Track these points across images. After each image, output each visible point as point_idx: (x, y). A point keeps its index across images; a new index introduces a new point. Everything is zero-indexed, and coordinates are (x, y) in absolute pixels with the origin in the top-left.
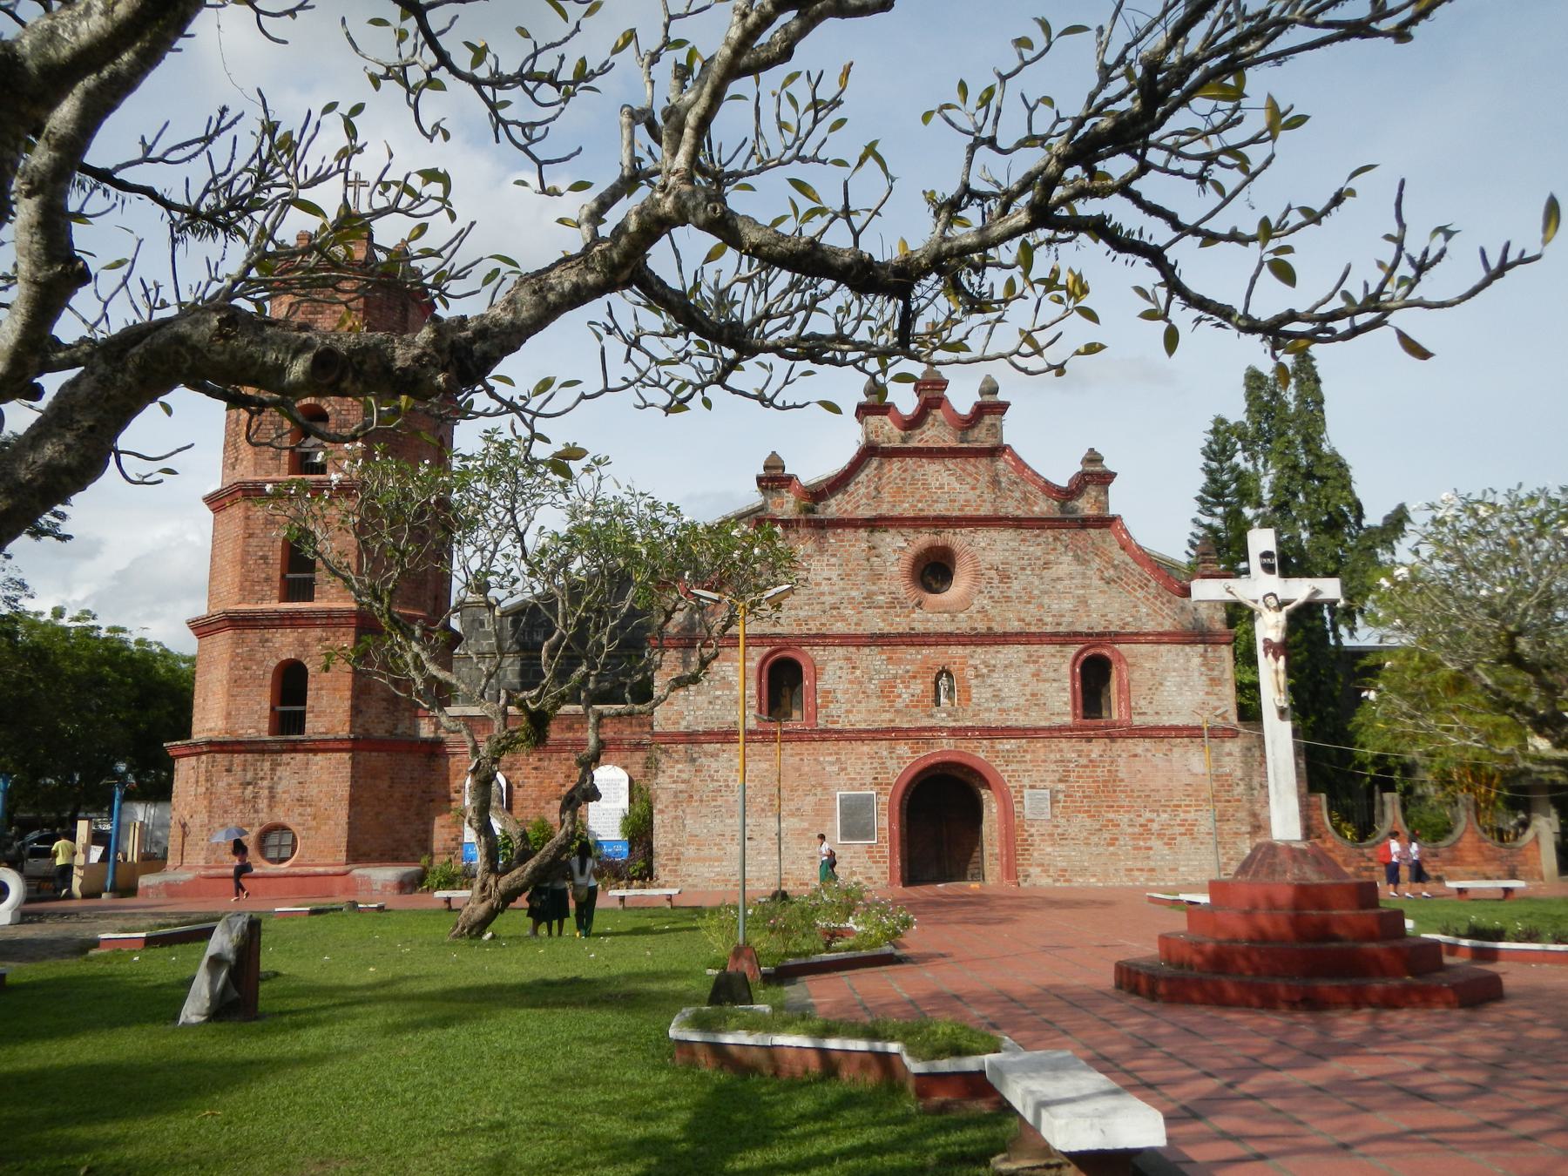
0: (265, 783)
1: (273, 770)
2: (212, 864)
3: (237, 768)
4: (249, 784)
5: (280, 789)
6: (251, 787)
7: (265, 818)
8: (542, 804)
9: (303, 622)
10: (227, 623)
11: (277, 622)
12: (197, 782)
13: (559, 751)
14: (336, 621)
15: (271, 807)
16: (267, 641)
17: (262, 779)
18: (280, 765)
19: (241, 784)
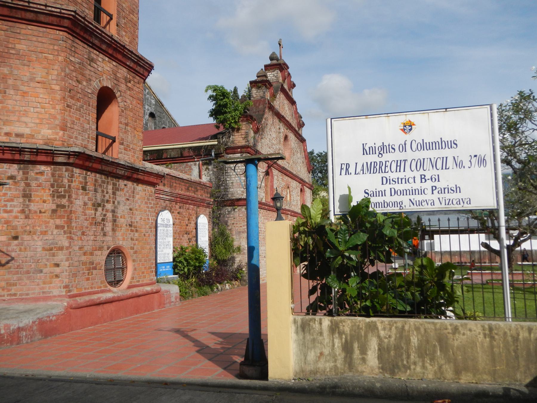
0: (109, 206)
1: (114, 193)
2: (75, 292)
3: (90, 187)
4: (99, 205)
5: (119, 213)
6: (100, 209)
7: (110, 242)
8: (181, 237)
9: (119, 57)
10: (66, 23)
11: (104, 47)
12: (27, 196)
13: (186, 203)
14: (138, 69)
15: (113, 230)
16: (92, 60)
17: (108, 201)
18: (117, 189)
19: (94, 205)
